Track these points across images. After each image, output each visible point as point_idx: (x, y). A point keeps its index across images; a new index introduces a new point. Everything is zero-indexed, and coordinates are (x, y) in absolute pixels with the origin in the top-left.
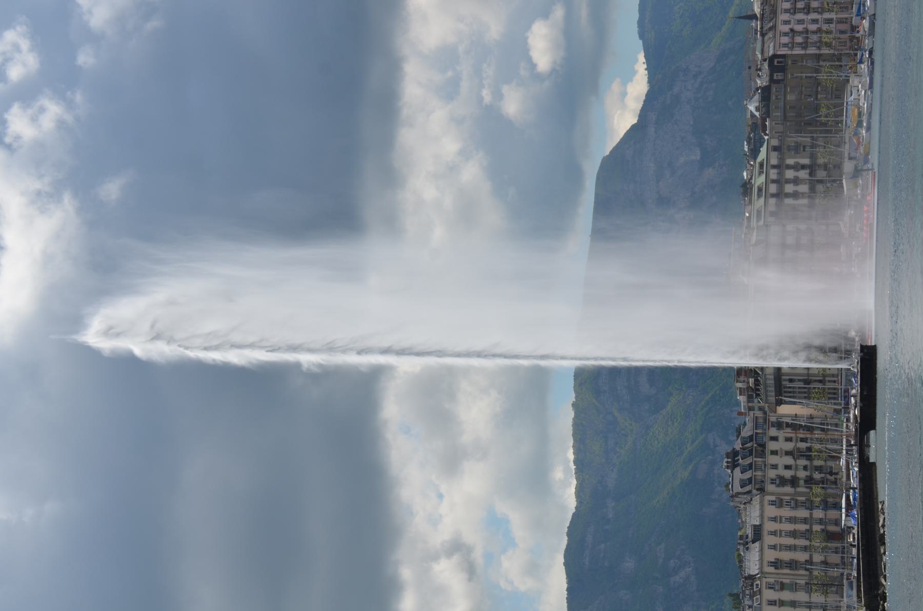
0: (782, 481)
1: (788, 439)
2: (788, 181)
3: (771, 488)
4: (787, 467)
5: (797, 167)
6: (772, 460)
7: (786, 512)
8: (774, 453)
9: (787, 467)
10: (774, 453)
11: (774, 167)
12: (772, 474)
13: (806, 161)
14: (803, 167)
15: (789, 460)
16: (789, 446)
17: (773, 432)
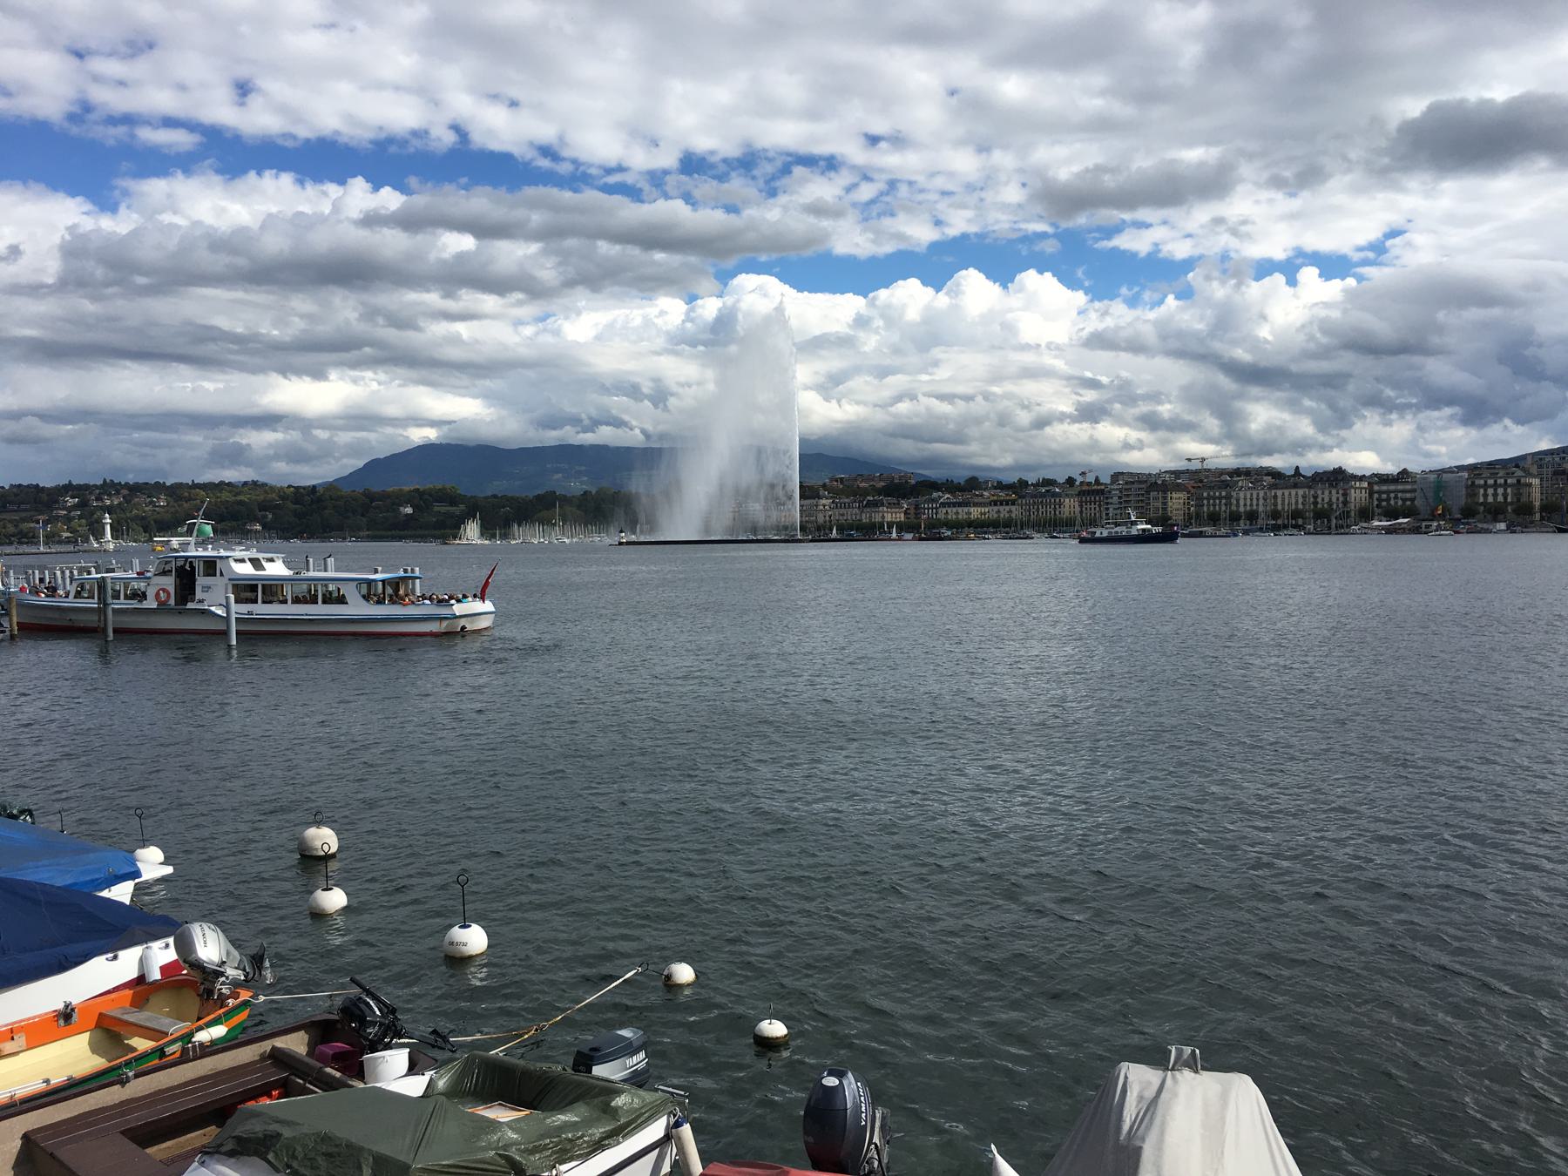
0: (1315, 497)
1: (1338, 499)
2: (1495, 490)
3: (1312, 492)
4: (1323, 499)
5: (1505, 495)
6: (1327, 492)
7: (1300, 500)
8: (1330, 492)
9: (1323, 499)
10: (1330, 492)
11: (1506, 481)
12: (1319, 492)
13: (1509, 499)
14: (1505, 498)
15: (1326, 500)
16: (1334, 500)
17: (1341, 492)
